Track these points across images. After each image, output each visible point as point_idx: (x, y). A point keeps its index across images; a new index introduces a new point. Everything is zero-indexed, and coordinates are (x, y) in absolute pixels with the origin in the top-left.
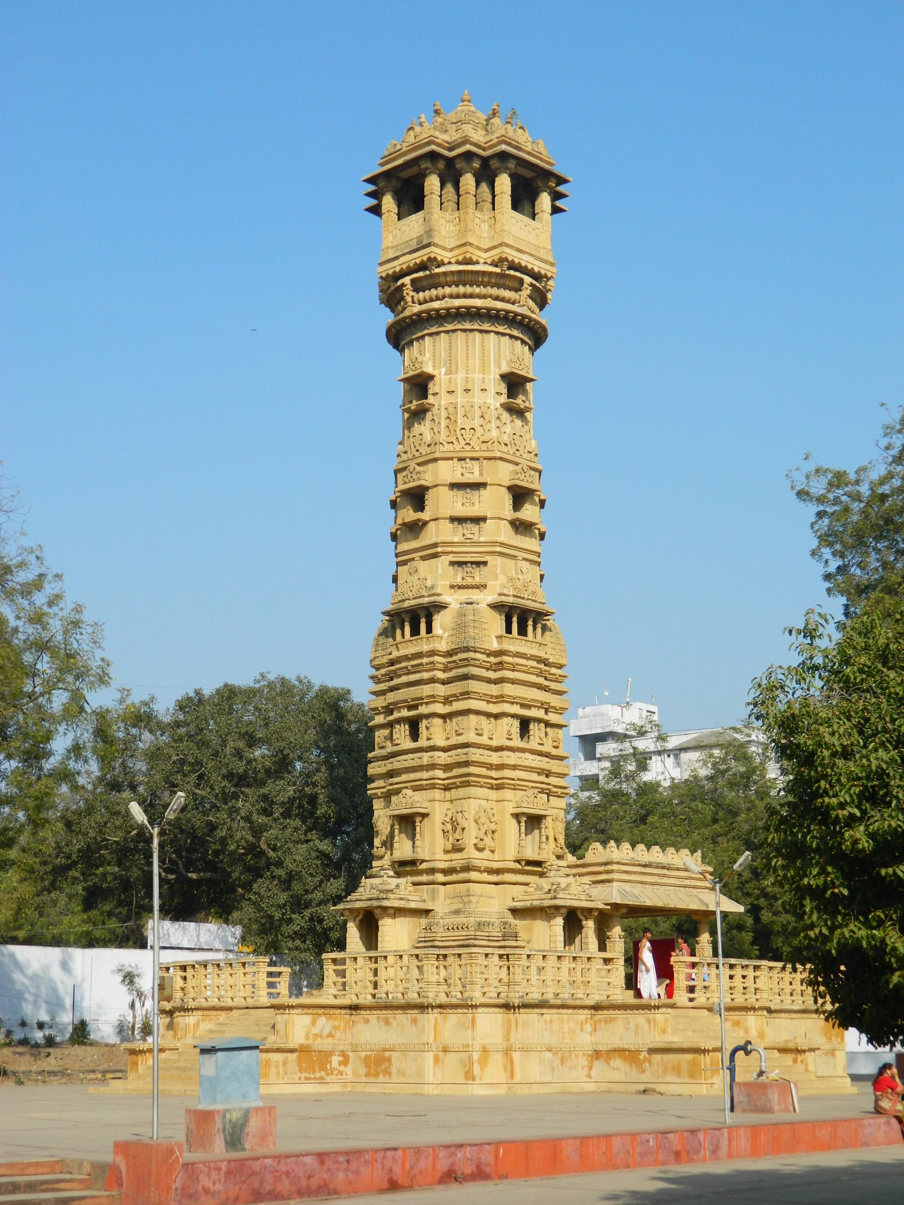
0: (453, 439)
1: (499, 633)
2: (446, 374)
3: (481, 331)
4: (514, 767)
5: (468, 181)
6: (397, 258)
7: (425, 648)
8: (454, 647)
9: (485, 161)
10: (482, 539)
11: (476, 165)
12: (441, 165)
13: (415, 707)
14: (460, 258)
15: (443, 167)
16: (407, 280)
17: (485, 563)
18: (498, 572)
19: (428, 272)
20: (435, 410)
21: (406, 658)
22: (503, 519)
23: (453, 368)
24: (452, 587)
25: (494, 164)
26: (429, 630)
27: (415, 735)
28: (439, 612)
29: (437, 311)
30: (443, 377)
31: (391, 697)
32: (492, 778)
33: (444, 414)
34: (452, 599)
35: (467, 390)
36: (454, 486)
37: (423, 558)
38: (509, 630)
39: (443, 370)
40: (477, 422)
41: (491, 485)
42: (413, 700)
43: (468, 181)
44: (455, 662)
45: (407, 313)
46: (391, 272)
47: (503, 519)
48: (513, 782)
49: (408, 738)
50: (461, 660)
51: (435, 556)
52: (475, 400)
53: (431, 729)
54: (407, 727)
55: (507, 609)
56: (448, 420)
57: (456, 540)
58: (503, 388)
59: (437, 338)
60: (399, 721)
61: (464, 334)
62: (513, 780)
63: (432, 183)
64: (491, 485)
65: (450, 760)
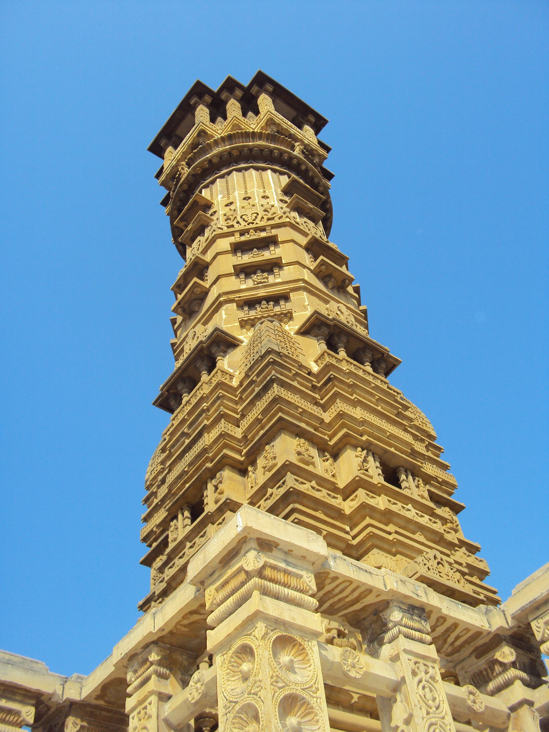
0: (234, 223)
1: (319, 352)
2: (223, 198)
3: (257, 169)
4: (388, 516)
7: (206, 390)
8: (249, 366)
9: (246, 91)
10: (279, 280)
11: (239, 93)
12: (208, 99)
15: (210, 101)
17: (286, 297)
18: (307, 303)
20: (212, 223)
22: (304, 267)
23: (231, 192)
24: (243, 324)
27: (196, 509)
28: (225, 352)
29: (210, 161)
30: (219, 200)
32: (347, 533)
33: (222, 219)
34: (245, 337)
35: (247, 198)
36: (238, 248)
37: (205, 324)
38: (332, 346)
39: (220, 196)
40: (262, 213)
41: (283, 242)
42: (190, 464)
45: (182, 179)
47: (304, 267)
48: (391, 537)
50: (258, 375)
51: (216, 310)
52: (257, 201)
53: (221, 486)
54: (187, 514)
55: (325, 330)
57: (243, 287)
58: (286, 199)
59: (214, 186)
61: (240, 174)
62: (390, 533)
64: (283, 242)
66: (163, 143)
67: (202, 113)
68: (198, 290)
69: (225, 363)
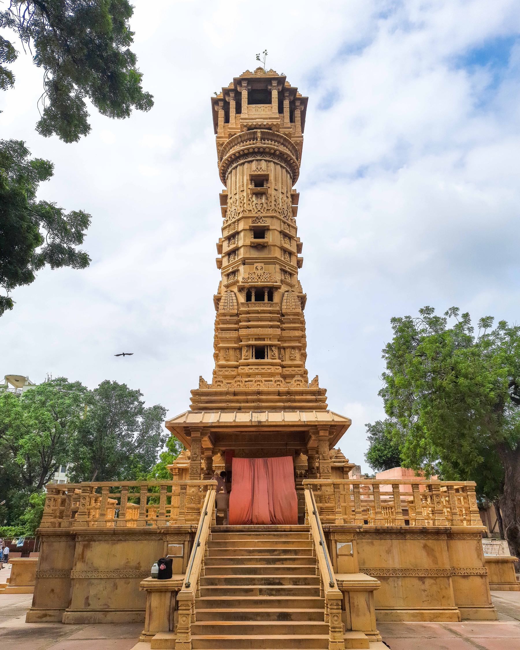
0: (280, 211)
5: (286, 103)
6: (255, 119)
13: (264, 339)
14: (287, 133)
16: (259, 130)
19: (271, 131)
21: (258, 312)
25: (298, 103)
26: (271, 299)
31: (243, 332)
43: (286, 103)
44: (290, 319)
46: (250, 124)
49: (254, 356)
50: (293, 319)
54: (254, 350)
56: (275, 203)
60: (248, 346)
63: (275, 94)
65: (288, 373)
66: (244, 84)
67: (275, 94)
68: (266, 244)
69: (276, 298)
